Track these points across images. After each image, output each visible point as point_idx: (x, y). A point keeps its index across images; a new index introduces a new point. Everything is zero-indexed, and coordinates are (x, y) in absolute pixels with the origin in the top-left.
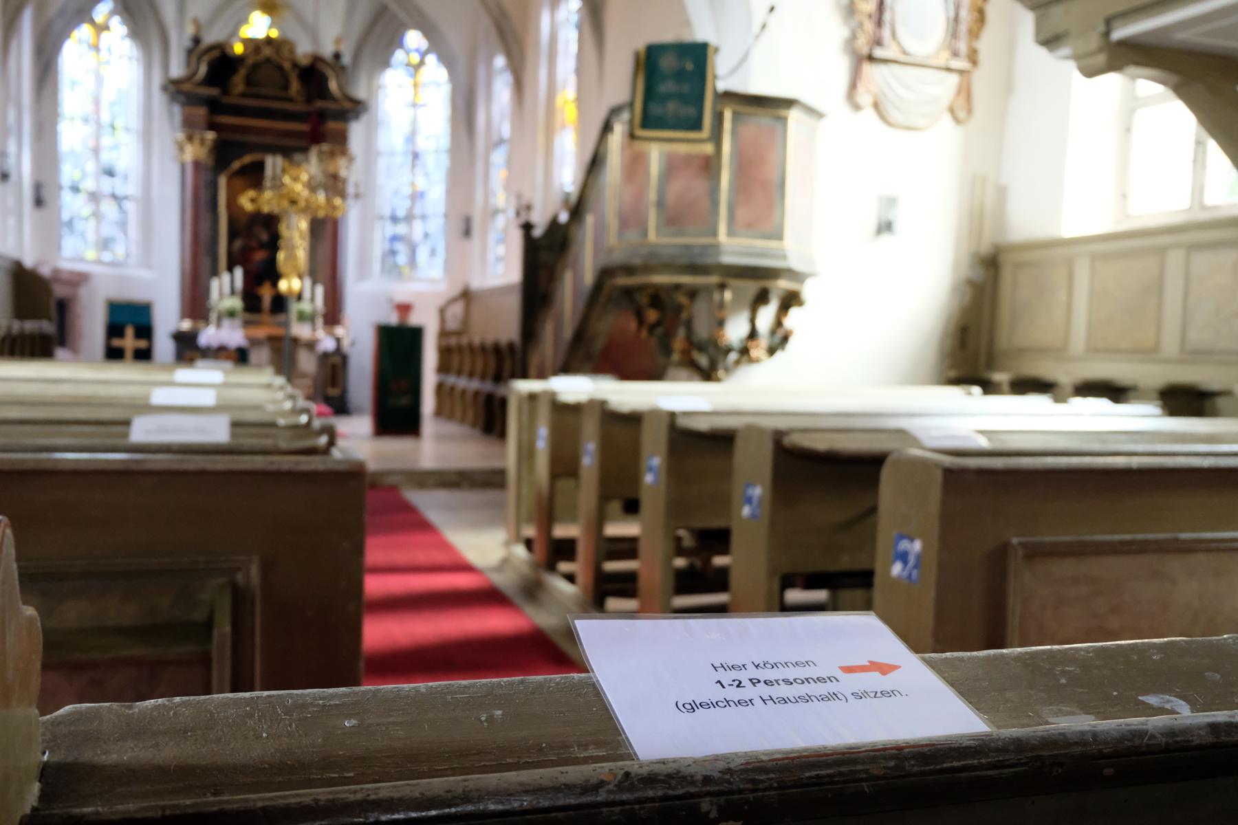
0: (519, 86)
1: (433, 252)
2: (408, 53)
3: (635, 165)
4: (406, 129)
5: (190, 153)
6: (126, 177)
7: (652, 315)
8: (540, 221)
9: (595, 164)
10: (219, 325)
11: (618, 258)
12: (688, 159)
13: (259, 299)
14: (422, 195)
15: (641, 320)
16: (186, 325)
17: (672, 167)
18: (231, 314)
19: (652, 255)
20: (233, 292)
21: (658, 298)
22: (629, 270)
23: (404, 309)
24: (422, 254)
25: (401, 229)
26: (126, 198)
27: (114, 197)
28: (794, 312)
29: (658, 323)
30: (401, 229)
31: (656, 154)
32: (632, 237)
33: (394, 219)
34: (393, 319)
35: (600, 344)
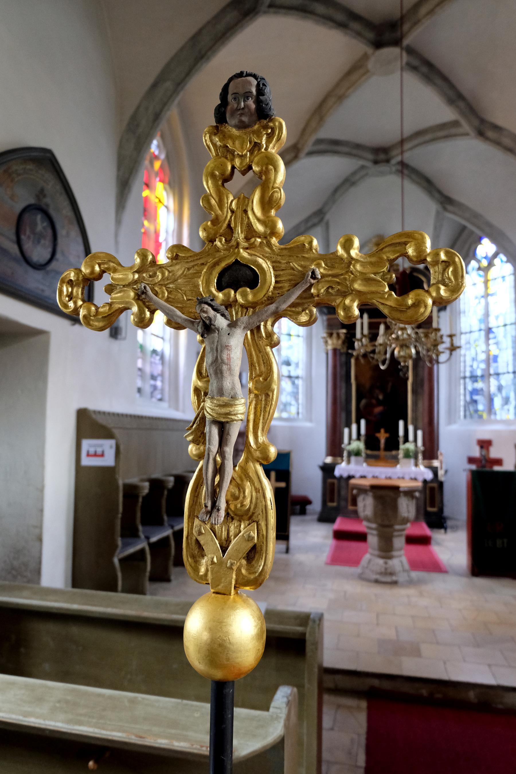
1: (506, 401)
2: (479, 261)
4: (480, 312)
5: (332, 343)
6: (297, 365)
10: (349, 462)
13: (378, 441)
14: (496, 358)
16: (329, 460)
18: (357, 453)
20: (359, 438)
23: (485, 444)
24: (498, 402)
25: (480, 385)
26: (297, 377)
27: (290, 377)
30: (480, 385)
33: (474, 378)
34: (476, 452)
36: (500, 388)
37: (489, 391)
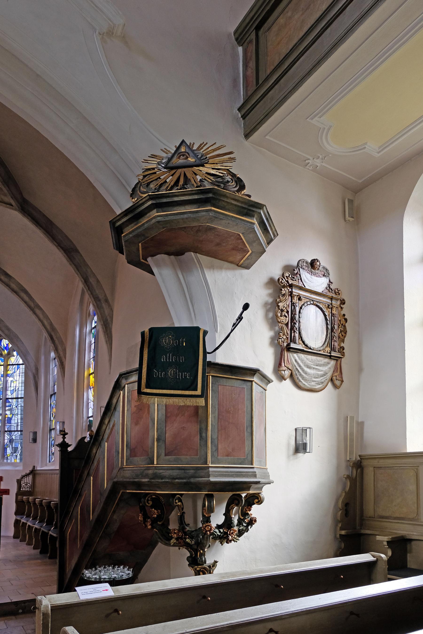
0: (62, 366)
3: (141, 412)
7: (155, 513)
8: (72, 442)
9: (109, 409)
11: (127, 475)
12: (181, 409)
15: (146, 517)
17: (169, 414)
19: (156, 476)
21: (157, 502)
22: (139, 485)
28: (255, 507)
29: (159, 518)
31: (157, 405)
32: (140, 461)
35: (115, 527)
36: (11, 441)
37: (4, 443)
